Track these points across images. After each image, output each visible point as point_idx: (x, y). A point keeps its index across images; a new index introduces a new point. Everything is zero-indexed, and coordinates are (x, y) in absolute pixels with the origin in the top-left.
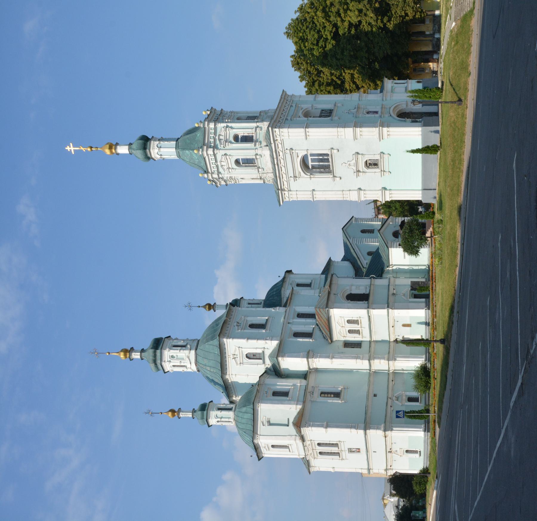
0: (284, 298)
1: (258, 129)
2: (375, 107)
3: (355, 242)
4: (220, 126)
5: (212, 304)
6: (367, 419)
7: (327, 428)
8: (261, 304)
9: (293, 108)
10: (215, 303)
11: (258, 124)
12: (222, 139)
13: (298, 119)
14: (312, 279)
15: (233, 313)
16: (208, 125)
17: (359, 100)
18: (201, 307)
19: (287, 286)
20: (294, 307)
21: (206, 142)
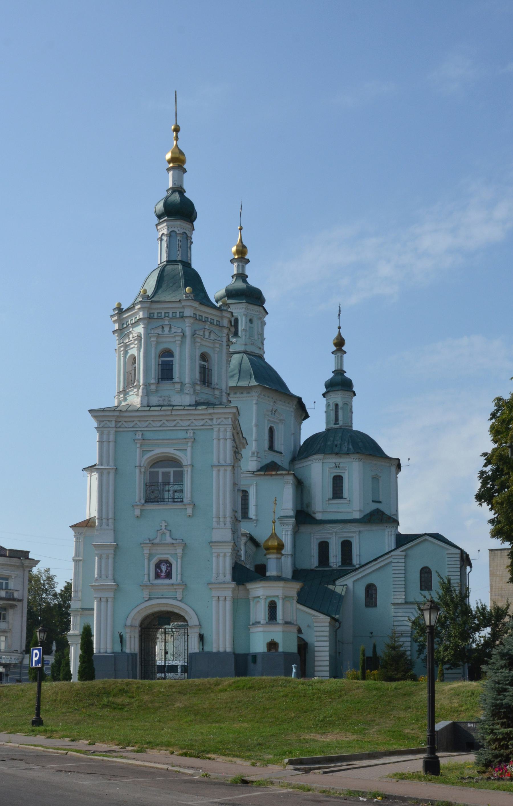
0: (310, 460)
1: (136, 390)
2: (179, 572)
3: (396, 561)
4: (140, 329)
5: (343, 348)
6: (87, 612)
7: (74, 561)
8: (335, 424)
9: (181, 435)
10: (345, 353)
11: (142, 387)
12: (129, 338)
13: (138, 450)
14: (348, 499)
15: (245, 395)
16: (139, 309)
17: (212, 542)
18: (339, 331)
19: (334, 460)
20: (255, 482)
21: (125, 316)
